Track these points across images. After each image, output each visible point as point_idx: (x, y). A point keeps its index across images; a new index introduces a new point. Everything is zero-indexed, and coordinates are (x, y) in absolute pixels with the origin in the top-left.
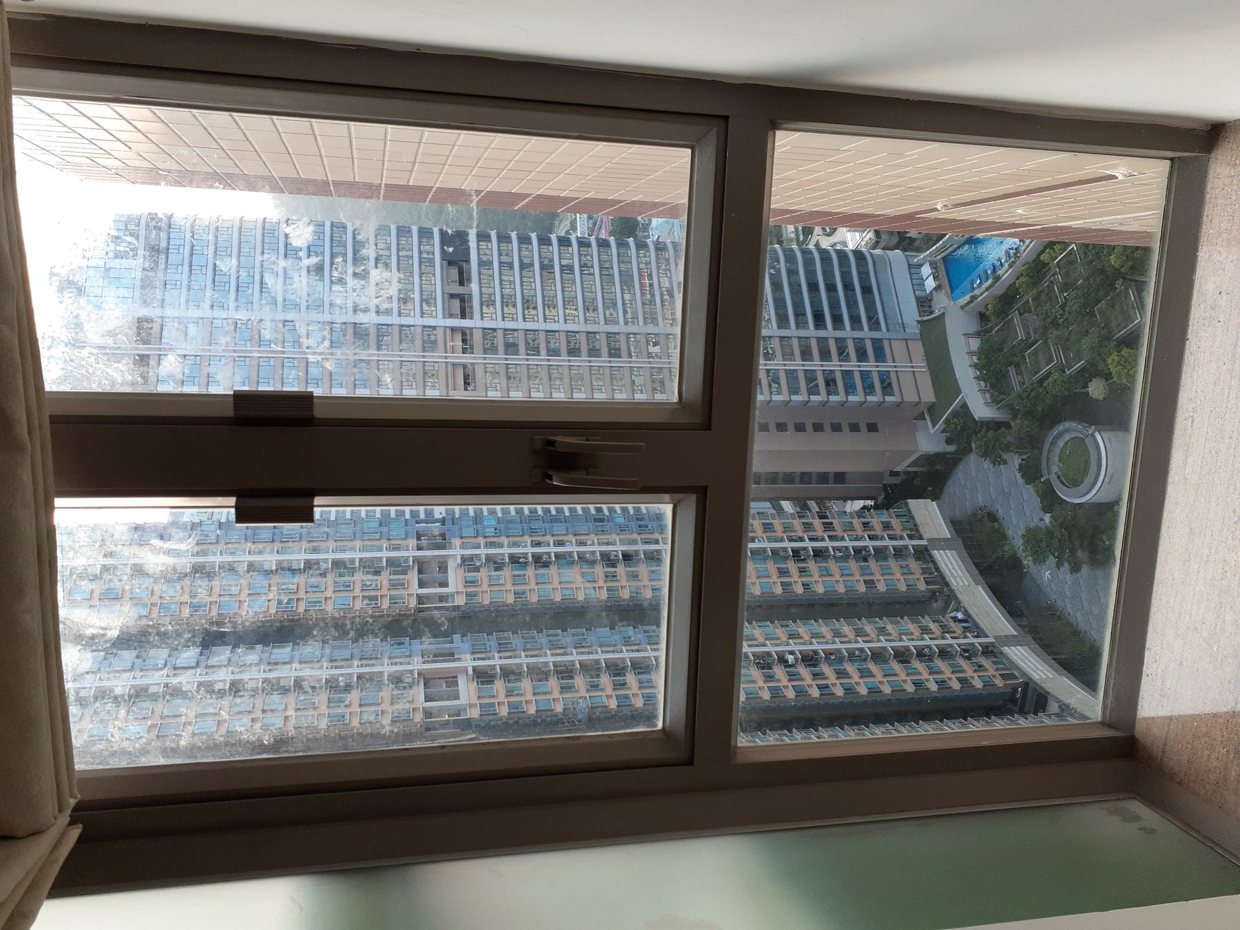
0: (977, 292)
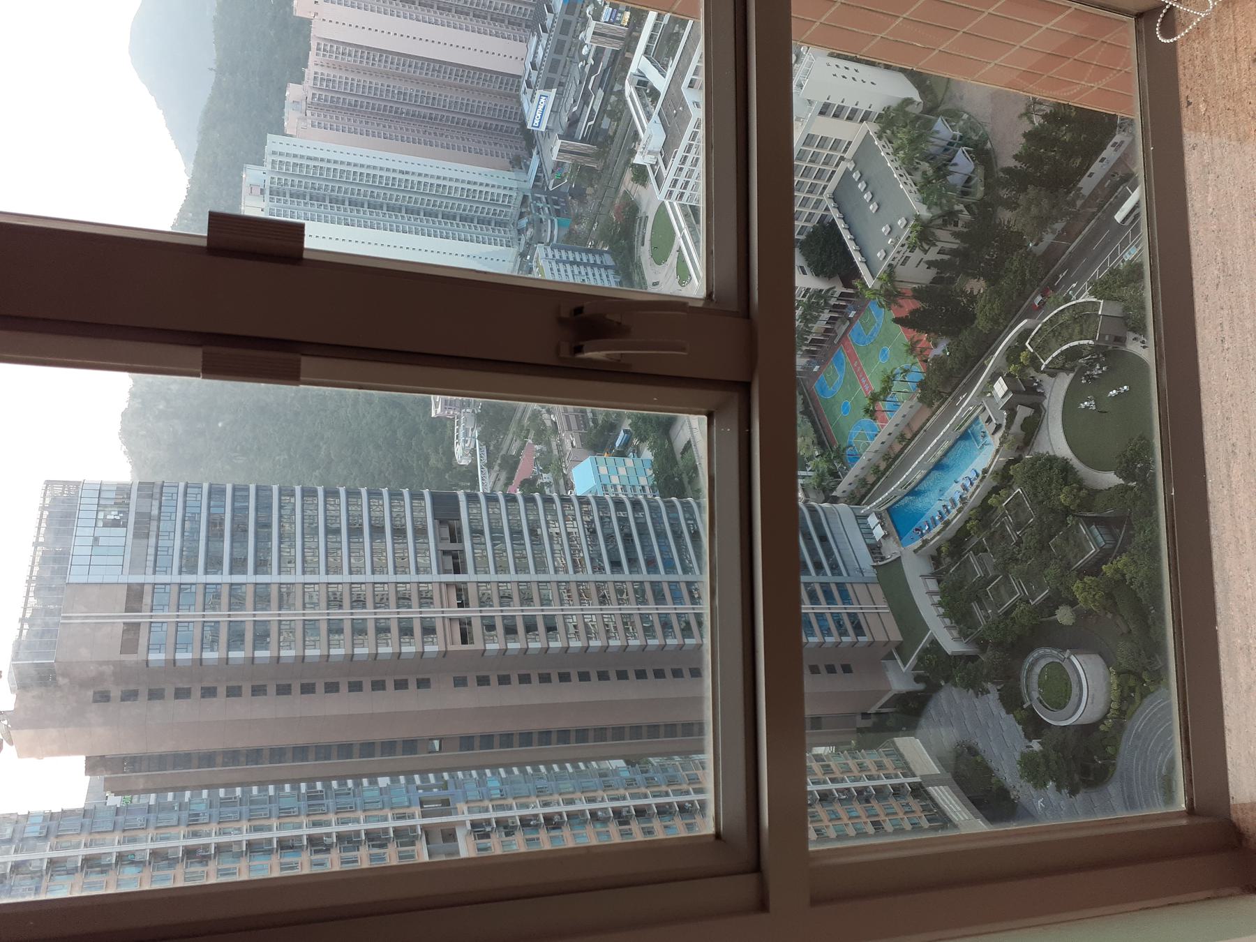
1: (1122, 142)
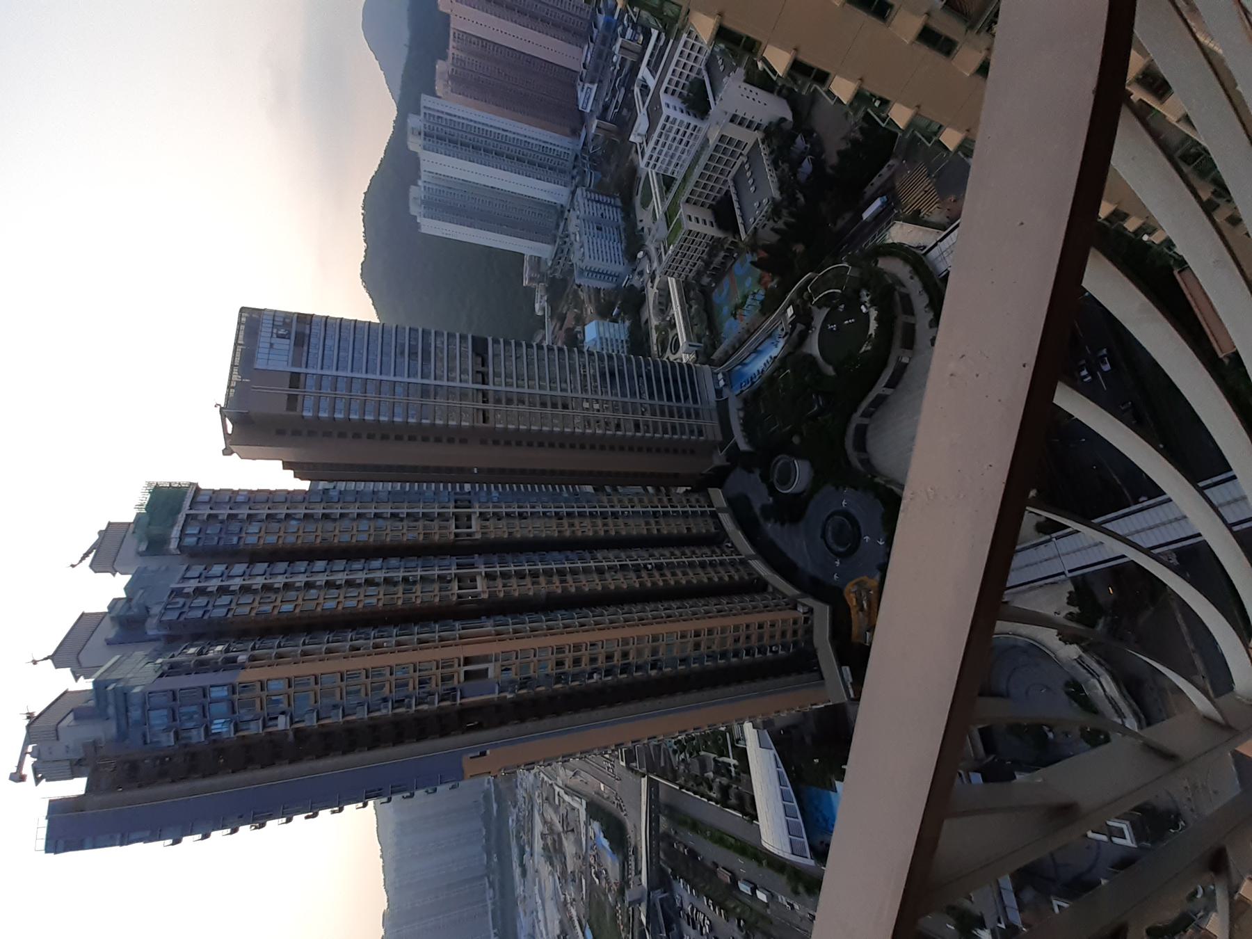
0: (743, 389)
1: (894, 165)
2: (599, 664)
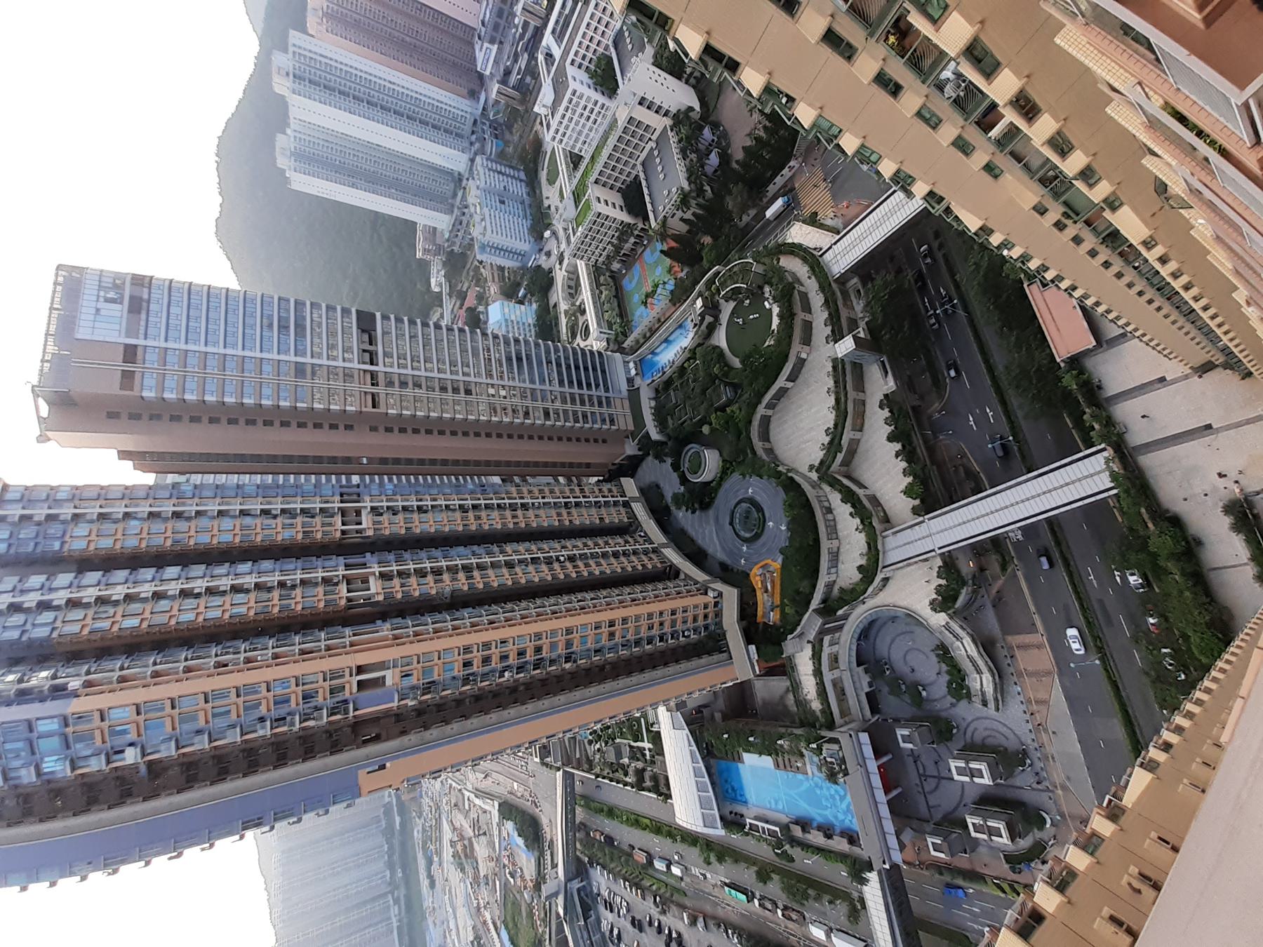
2: (511, 661)
